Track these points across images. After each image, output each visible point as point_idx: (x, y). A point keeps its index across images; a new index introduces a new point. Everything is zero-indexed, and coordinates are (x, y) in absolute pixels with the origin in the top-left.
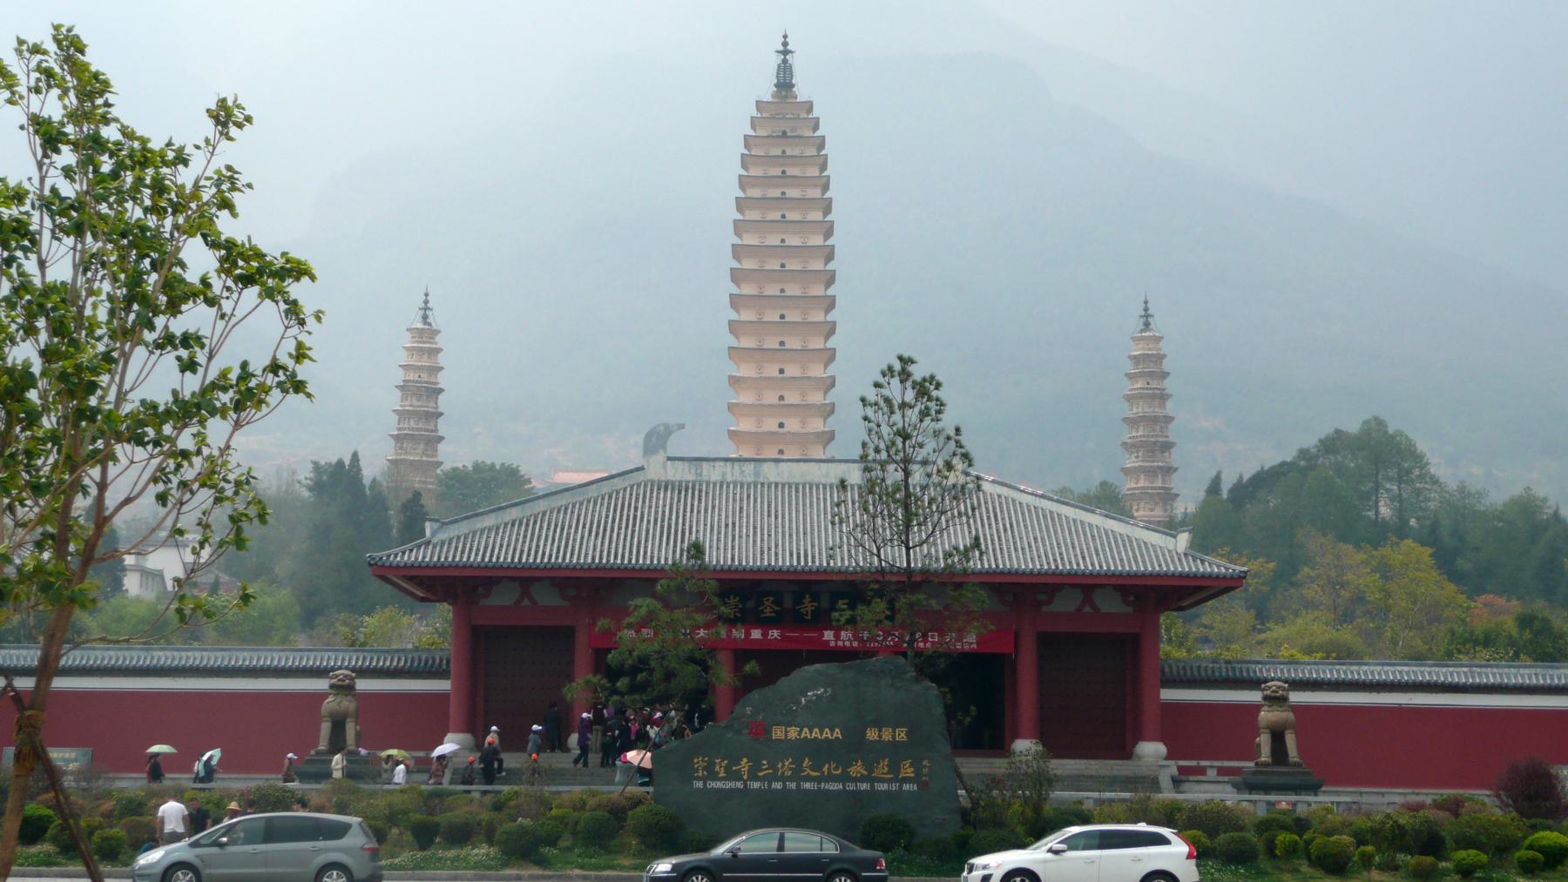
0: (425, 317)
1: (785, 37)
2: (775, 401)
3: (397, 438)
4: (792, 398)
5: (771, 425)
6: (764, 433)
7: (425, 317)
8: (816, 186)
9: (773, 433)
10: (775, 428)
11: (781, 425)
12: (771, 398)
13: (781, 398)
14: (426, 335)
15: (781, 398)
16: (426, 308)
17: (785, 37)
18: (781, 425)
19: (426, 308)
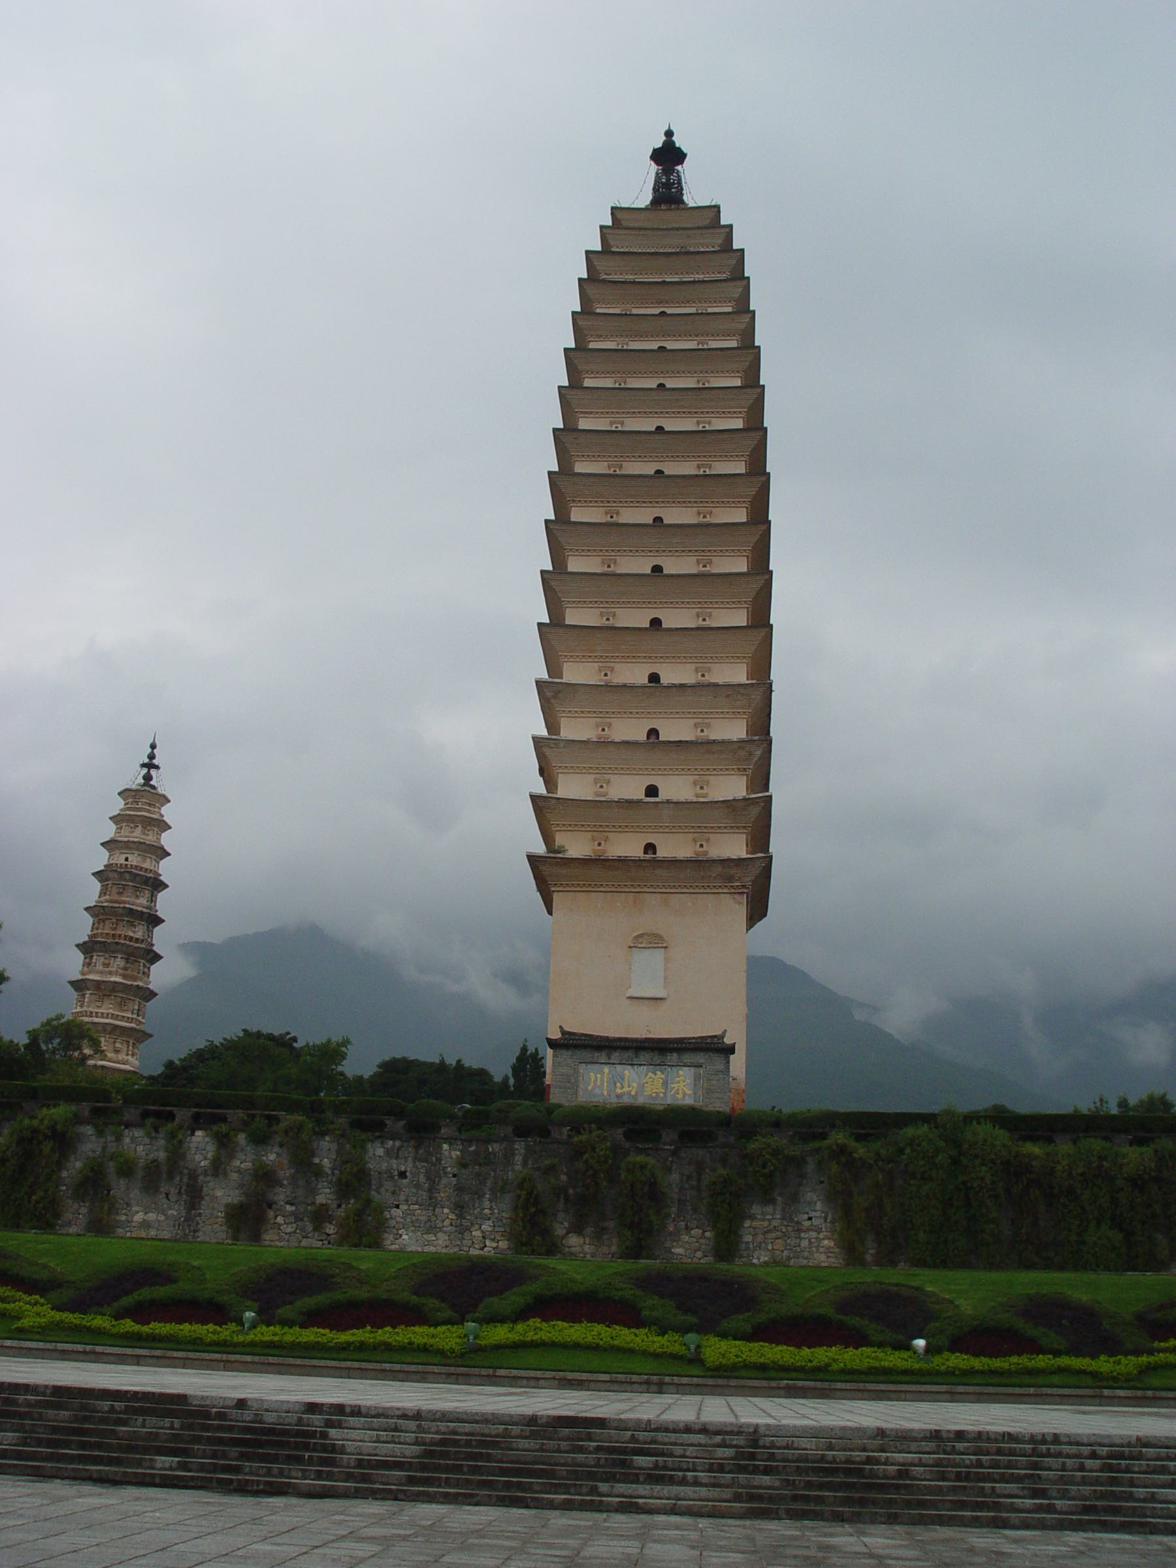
0: (148, 778)
1: (669, 134)
2: (643, 737)
3: (87, 948)
4: (675, 730)
5: (630, 787)
6: (610, 803)
7: (148, 778)
8: (729, 334)
9: (630, 803)
10: (640, 794)
11: (652, 791)
12: (632, 730)
13: (653, 733)
14: (142, 807)
15: (653, 733)
16: (150, 765)
17: (669, 134)
18: (652, 791)
19: (150, 765)
